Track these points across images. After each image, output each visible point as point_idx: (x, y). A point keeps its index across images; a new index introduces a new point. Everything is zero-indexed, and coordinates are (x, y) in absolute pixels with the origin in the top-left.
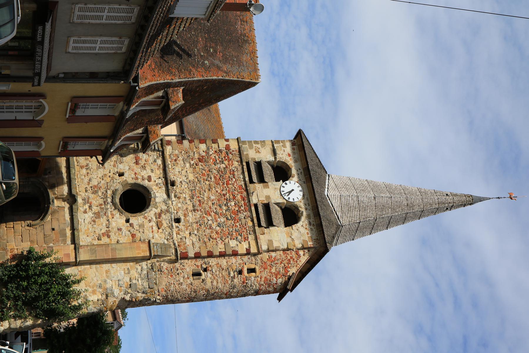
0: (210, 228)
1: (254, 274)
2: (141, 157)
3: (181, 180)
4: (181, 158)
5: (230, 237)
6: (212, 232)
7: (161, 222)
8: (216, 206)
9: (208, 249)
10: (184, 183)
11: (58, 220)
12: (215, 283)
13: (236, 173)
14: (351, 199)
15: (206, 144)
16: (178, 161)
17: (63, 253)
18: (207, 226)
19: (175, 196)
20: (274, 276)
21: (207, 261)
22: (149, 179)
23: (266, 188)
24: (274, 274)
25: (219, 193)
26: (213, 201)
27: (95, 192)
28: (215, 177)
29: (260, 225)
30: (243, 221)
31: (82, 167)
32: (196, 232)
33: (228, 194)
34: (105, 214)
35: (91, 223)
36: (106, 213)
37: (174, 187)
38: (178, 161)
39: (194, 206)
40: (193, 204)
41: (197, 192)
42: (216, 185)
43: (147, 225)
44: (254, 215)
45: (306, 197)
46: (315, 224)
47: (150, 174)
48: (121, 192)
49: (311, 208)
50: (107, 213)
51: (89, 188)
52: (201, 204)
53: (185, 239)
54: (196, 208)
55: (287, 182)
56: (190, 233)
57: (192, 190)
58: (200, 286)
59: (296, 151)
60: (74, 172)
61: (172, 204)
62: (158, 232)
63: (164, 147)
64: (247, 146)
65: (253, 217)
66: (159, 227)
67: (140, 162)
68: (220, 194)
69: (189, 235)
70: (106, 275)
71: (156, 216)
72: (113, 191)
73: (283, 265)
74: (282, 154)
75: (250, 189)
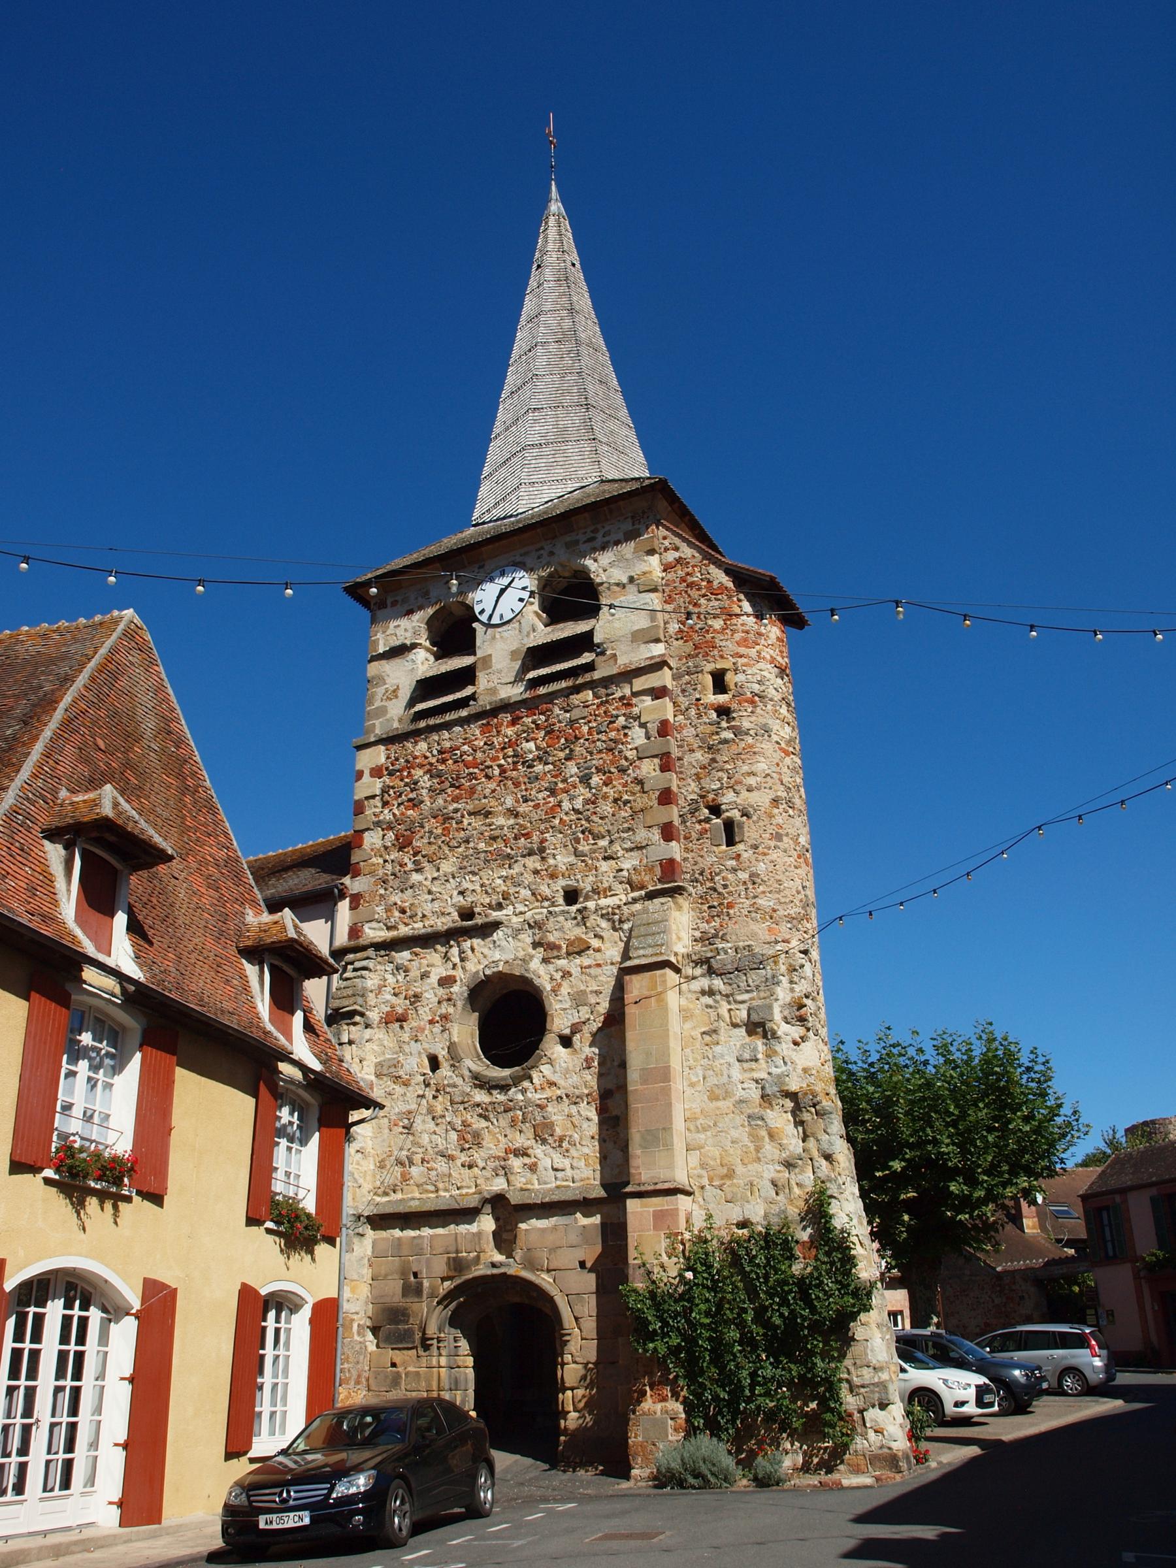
0: (593, 803)
1: (730, 678)
2: (388, 1009)
3: (455, 893)
4: (396, 898)
5: (620, 746)
6: (605, 797)
7: (570, 943)
8: (533, 792)
9: (655, 802)
10: (465, 885)
11: (553, 1250)
12: (752, 781)
13: (447, 745)
14: (534, 462)
15: (368, 829)
16: (407, 904)
17: (651, 1233)
18: (589, 813)
19: (500, 906)
20: (734, 621)
21: (688, 808)
22: (445, 982)
23: (491, 660)
24: (728, 622)
25: (498, 786)
26: (517, 801)
27: (478, 1139)
28: (456, 799)
29: (590, 667)
30: (576, 713)
31: (405, 1178)
32: (603, 843)
33: (502, 762)
34: (541, 1107)
35: (567, 1151)
36: (538, 1106)
37: (477, 910)
38: (407, 904)
39: (531, 853)
40: (524, 856)
41: (491, 845)
42: (476, 796)
43: (577, 982)
44: (564, 684)
45: (518, 559)
46: (593, 528)
47: (434, 979)
48: (483, 1062)
49: (549, 542)
50: (539, 1102)
51: (463, 1158)
52: (525, 831)
53: (622, 870)
54: (535, 846)
55: (477, 609)
56: (605, 858)
57: (486, 861)
58: (761, 824)
59: (399, 598)
60: (417, 1203)
61: (521, 913)
62: (598, 950)
63: (366, 943)
64: (377, 722)
65: (567, 688)
66: (585, 946)
67: (400, 1011)
68: (501, 781)
69: (612, 862)
70: (724, 1099)
71: (554, 958)
72: (476, 1086)
73: (703, 601)
74: (406, 630)
75: (490, 704)
